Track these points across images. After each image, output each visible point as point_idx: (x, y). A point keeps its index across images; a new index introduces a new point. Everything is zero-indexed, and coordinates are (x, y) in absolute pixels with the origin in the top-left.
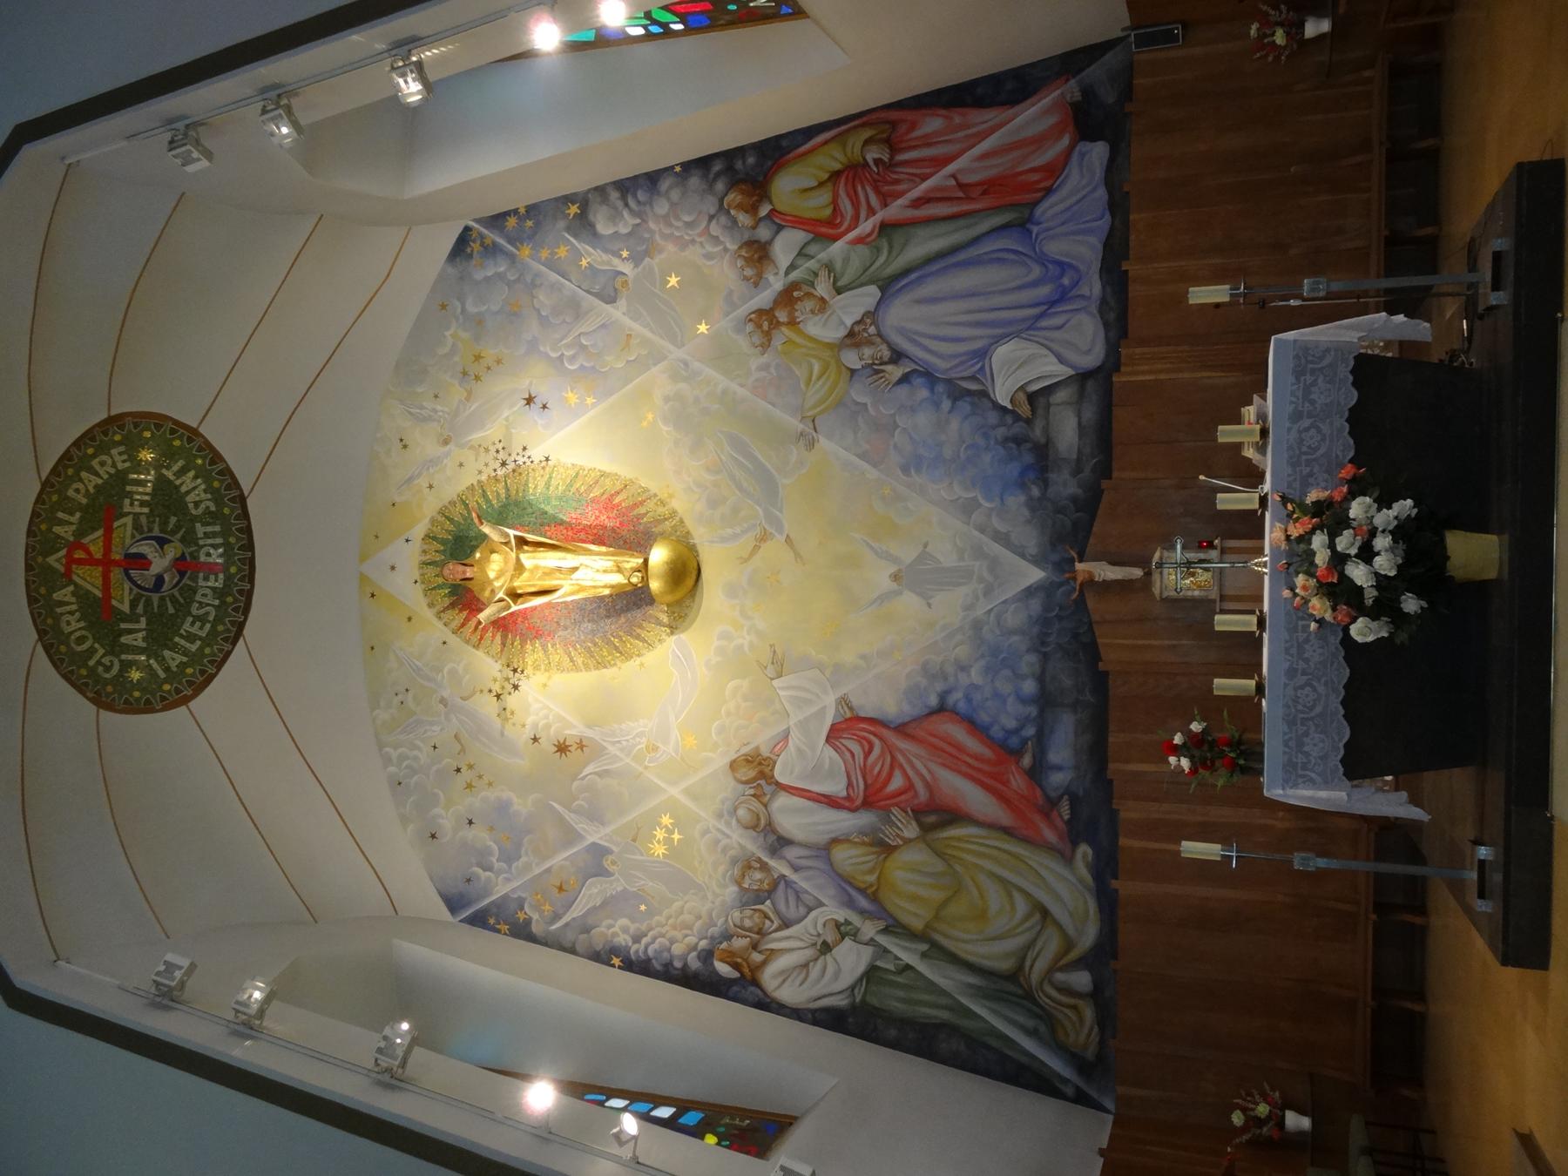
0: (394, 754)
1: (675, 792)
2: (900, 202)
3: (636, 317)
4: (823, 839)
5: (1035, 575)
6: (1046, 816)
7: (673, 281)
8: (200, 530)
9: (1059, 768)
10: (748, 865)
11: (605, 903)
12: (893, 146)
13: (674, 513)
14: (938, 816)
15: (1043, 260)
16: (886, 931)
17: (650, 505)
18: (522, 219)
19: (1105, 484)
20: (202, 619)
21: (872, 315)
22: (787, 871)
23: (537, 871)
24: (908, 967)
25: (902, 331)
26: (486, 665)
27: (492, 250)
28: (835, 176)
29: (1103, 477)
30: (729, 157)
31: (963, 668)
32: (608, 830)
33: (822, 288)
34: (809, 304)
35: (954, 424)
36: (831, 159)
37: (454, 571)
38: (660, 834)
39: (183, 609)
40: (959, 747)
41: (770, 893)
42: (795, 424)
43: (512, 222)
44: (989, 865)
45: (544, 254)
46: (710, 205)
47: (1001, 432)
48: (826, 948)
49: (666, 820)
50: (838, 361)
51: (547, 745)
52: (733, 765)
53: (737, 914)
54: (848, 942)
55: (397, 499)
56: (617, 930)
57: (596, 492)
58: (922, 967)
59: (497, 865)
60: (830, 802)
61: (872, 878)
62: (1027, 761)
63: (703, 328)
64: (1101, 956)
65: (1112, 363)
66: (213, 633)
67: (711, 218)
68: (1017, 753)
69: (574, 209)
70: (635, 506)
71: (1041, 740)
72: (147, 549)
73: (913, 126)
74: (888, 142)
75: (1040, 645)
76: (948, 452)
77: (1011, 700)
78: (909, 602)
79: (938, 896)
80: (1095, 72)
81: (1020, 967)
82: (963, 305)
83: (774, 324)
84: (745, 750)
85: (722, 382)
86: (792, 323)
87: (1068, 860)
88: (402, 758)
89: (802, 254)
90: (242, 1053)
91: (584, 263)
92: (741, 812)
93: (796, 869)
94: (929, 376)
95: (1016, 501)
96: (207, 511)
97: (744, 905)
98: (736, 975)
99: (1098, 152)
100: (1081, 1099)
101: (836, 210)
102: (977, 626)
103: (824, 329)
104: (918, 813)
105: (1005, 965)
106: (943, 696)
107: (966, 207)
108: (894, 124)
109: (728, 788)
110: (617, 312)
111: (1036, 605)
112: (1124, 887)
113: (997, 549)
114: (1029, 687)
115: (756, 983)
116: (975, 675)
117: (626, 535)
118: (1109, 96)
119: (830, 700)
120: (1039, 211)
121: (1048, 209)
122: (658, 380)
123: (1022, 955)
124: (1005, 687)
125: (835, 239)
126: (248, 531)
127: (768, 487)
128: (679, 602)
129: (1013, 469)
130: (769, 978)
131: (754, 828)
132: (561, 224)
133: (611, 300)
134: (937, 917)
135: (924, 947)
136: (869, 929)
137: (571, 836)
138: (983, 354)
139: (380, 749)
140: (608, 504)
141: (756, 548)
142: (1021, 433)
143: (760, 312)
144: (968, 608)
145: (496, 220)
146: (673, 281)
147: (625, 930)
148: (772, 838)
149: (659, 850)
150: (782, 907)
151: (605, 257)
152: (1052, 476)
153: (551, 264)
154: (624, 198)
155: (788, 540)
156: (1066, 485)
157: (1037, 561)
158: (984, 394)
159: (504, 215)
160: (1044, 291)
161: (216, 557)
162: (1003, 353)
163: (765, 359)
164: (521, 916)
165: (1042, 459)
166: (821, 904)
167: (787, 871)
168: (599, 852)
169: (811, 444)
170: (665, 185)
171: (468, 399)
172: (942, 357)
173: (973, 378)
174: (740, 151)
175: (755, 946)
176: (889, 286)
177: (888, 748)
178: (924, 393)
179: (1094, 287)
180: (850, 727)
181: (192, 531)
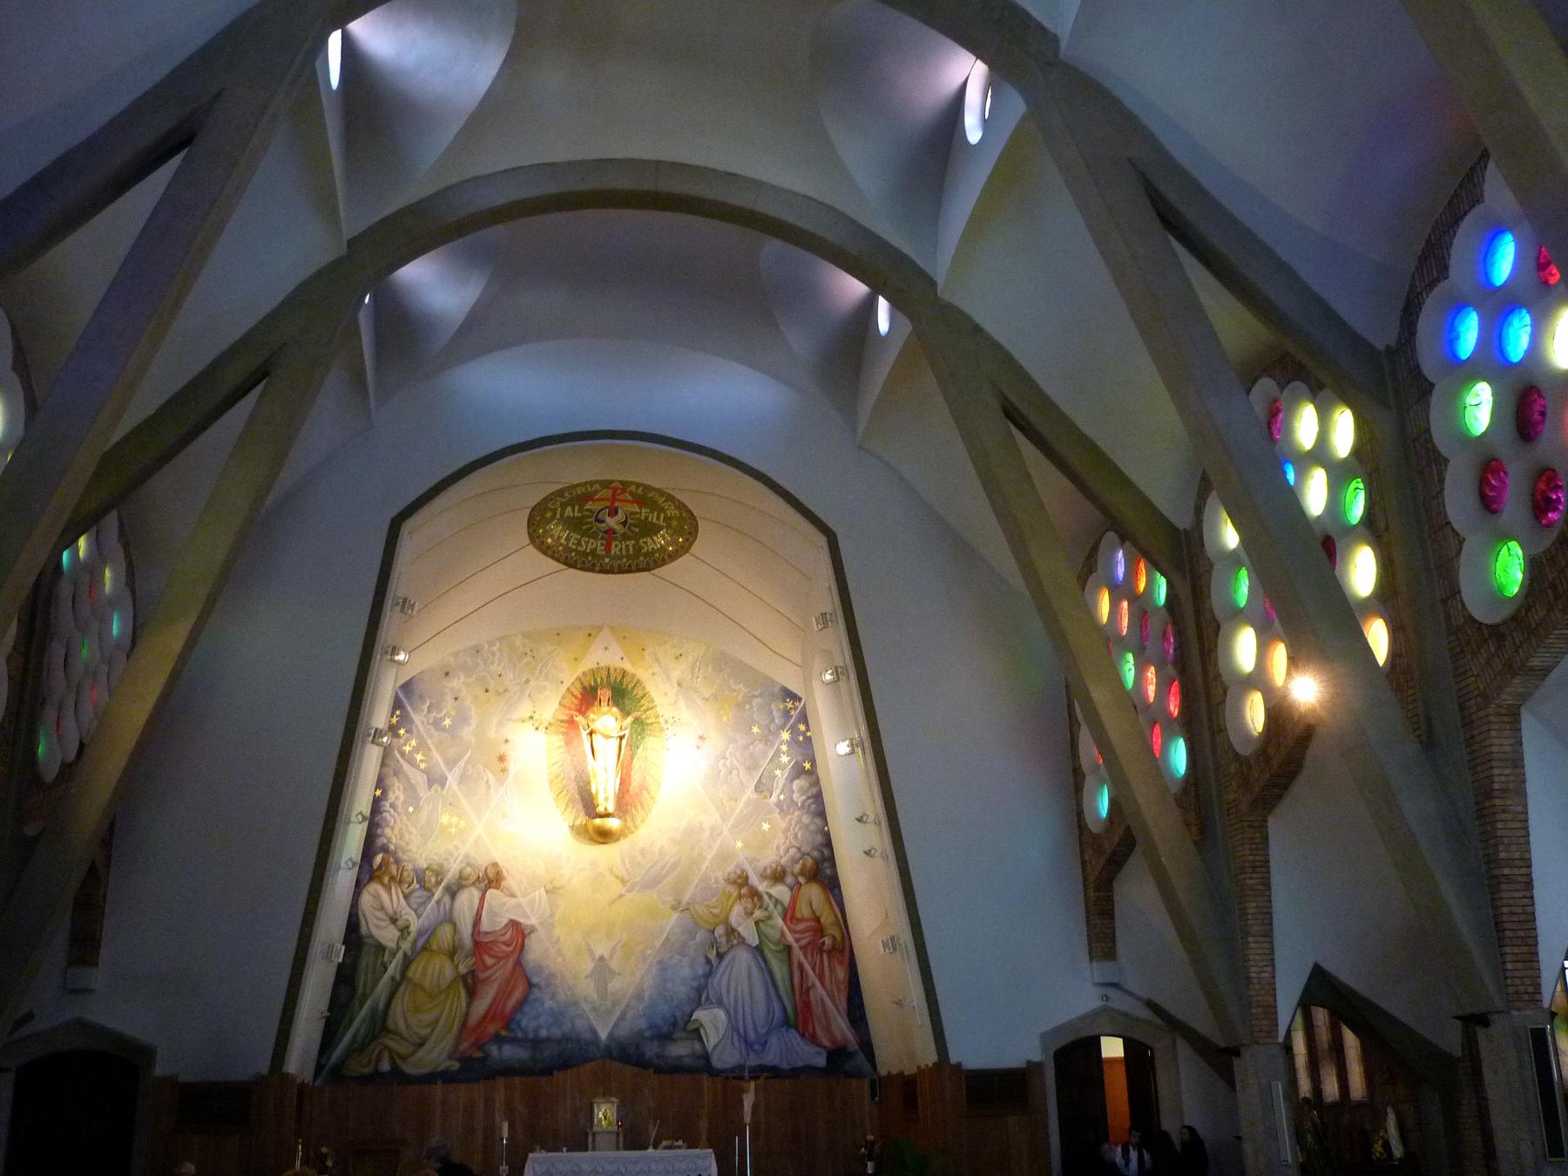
1: (479, 830)
3: (747, 804)
6: (474, 1044)
7: (766, 826)
9: (500, 1049)
10: (439, 873)
13: (637, 827)
14: (471, 984)
16: (405, 955)
18: (804, 734)
20: (579, 544)
21: (743, 941)
22: (436, 896)
24: (386, 970)
26: (550, 706)
27: (786, 714)
28: (818, 920)
29: (654, 1071)
30: (831, 859)
31: (553, 996)
33: (758, 914)
34: (749, 906)
36: (827, 918)
37: (604, 694)
38: (455, 820)
39: (585, 534)
40: (510, 994)
41: (423, 887)
42: (686, 897)
43: (802, 728)
45: (784, 748)
46: (806, 849)
47: (679, 1014)
48: (394, 921)
51: (503, 749)
52: (495, 865)
53: (410, 867)
54: (397, 933)
56: (397, 794)
57: (649, 779)
58: (387, 976)
60: (477, 922)
61: (435, 947)
62: (504, 1033)
63: (739, 844)
64: (398, 1075)
66: (572, 550)
68: (507, 1026)
69: (807, 766)
71: (513, 1040)
72: (621, 516)
73: (841, 963)
74: (834, 948)
75: (566, 1039)
76: (669, 985)
78: (589, 966)
79: (427, 985)
80: (861, 1058)
81: (389, 1032)
83: (740, 886)
84: (504, 873)
87: (450, 1057)
88: (493, 654)
89: (777, 902)
90: (377, 656)
91: (778, 772)
92: (469, 870)
93: (438, 902)
94: (709, 975)
95: (642, 1024)
96: (641, 548)
97: (415, 870)
99: (821, 1061)
100: (319, 1068)
102: (576, 1004)
103: (736, 915)
104: (472, 973)
105: (390, 1023)
106: (538, 986)
108: (842, 952)
109: (482, 861)
110: (750, 793)
111: (587, 1036)
112: (438, 1089)
114: (544, 1033)
115: (371, 879)
116: (549, 1003)
119: (533, 921)
120: (793, 1031)
121: (794, 1036)
122: (711, 818)
123: (396, 1033)
124: (542, 1020)
125: (784, 919)
126: (629, 571)
127: (651, 884)
128: (587, 831)
129: (660, 1022)
130: (374, 887)
131: (461, 877)
133: (757, 789)
135: (398, 977)
136: (406, 946)
137: (451, 764)
138: (720, 1003)
140: (643, 787)
141: (617, 877)
142: (678, 1025)
143: (747, 878)
145: (804, 718)
146: (766, 826)
149: (445, 819)
155: (622, 896)
156: (651, 1050)
157: (610, 1036)
158: (699, 1004)
159: (806, 723)
160: (752, 1036)
164: (402, 732)
165: (665, 1037)
167: (436, 896)
168: (442, 782)
169: (674, 908)
170: (818, 821)
172: (719, 981)
174: (834, 865)
175: (392, 878)
176: (759, 950)
177: (507, 956)
178: (700, 972)
179: (753, 1061)
180: (519, 932)
181: (629, 538)
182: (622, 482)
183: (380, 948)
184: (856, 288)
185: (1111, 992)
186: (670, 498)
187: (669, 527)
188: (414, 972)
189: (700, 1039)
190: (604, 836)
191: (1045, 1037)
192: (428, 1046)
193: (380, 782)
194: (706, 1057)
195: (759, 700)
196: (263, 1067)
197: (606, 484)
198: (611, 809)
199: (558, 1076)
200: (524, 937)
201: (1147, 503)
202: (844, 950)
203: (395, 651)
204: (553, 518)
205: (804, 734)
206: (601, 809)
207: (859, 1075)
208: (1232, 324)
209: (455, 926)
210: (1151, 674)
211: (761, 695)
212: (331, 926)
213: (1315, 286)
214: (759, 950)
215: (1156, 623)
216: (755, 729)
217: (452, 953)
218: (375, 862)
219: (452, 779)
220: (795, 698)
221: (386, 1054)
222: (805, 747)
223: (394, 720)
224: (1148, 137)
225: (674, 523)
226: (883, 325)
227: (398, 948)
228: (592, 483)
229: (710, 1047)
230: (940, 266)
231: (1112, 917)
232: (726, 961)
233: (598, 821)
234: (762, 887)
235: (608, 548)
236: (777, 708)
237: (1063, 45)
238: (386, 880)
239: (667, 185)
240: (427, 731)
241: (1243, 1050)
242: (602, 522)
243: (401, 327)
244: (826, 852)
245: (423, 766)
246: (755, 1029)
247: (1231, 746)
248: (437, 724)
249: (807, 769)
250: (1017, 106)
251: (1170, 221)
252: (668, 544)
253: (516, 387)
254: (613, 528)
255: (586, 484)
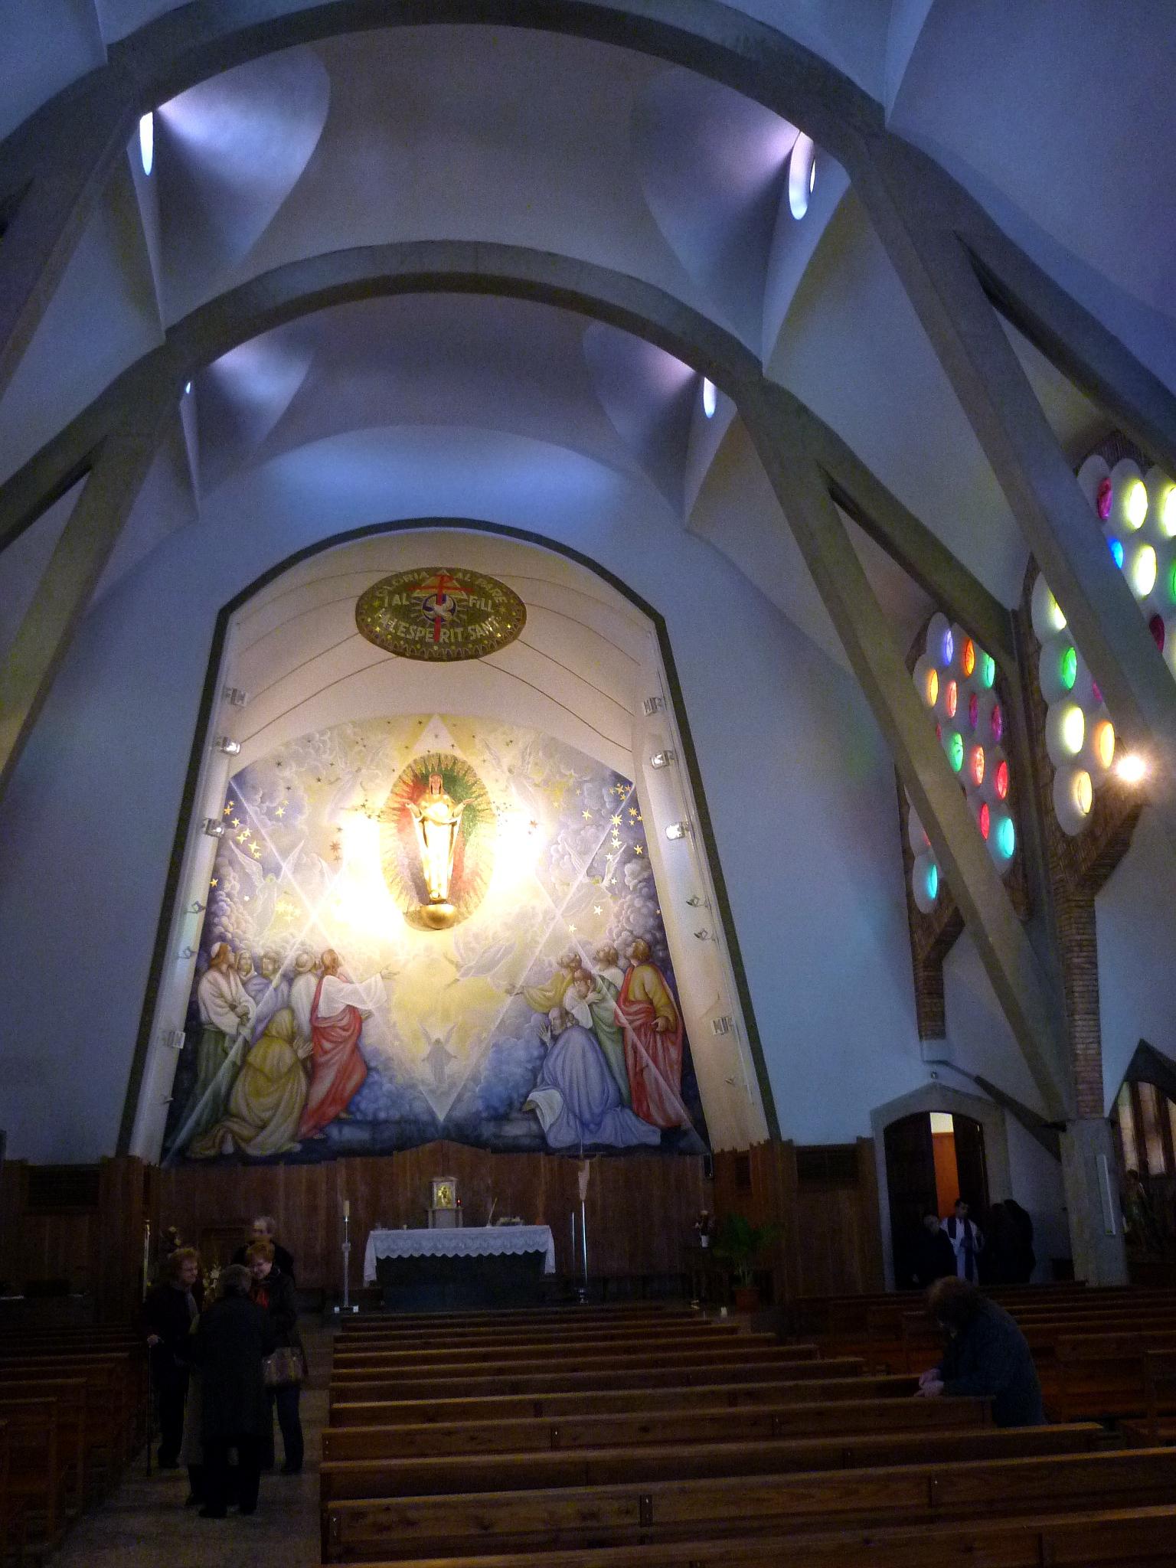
0: (326, 738)
2: (636, 1038)
4: (294, 1004)
5: (441, 1117)
6: (315, 1127)
7: (598, 910)
8: (459, 630)
9: (340, 1132)
10: (276, 961)
11: (247, 875)
12: (665, 1032)
13: (470, 913)
14: (311, 1068)
15: (603, 1113)
16: (246, 1041)
17: (475, 899)
18: (635, 818)
19: (489, 1150)
20: (407, 632)
21: (577, 1024)
22: (274, 983)
23: (263, 832)
24: (226, 1054)
25: (568, 1041)
27: (617, 799)
28: (651, 1002)
29: (490, 1147)
30: (663, 942)
31: (391, 1080)
32: (290, 876)
34: (583, 989)
35: (519, 1071)
36: (659, 1000)
37: (436, 781)
38: (290, 908)
40: (349, 1078)
41: (262, 975)
43: (633, 812)
44: (287, 1095)
45: (615, 832)
46: (638, 931)
47: (515, 1096)
48: (233, 1007)
49: (298, 912)
50: (551, 1007)
52: (331, 951)
54: (237, 1020)
55: (477, 740)
56: (232, 883)
58: (227, 1063)
59: (265, 806)
60: (315, 1008)
62: (343, 1115)
63: (572, 928)
64: (242, 1158)
65: (549, 1151)
67: (631, 932)
68: (347, 1110)
69: (639, 850)
70: (475, 890)
72: (449, 603)
73: (674, 1044)
75: (403, 1121)
76: (504, 1067)
77: (375, 1106)
78: (424, 1049)
79: (267, 1070)
80: (695, 1137)
82: (581, 1074)
83: (573, 970)
85: (543, 940)
86: (574, 980)
87: (293, 1138)
89: (610, 984)
90: (209, 748)
91: (609, 857)
92: (305, 957)
93: (275, 989)
94: (543, 1057)
95: (479, 1105)
98: (213, 955)
99: (655, 1139)
100: (165, 1151)
101: (633, 1003)
102: (413, 1086)
104: (311, 1058)
105: (232, 1106)
107: (631, 1073)
108: (675, 1032)
109: (318, 947)
110: (582, 877)
111: (425, 1118)
112: (281, 1170)
113: (454, 1096)
114: (382, 1115)
115: (210, 967)
116: (387, 1086)
117: (458, 887)
118: (682, 1144)
120: (628, 1111)
121: (628, 1116)
122: (543, 903)
124: (383, 1102)
126: (458, 658)
127: (485, 968)
128: (421, 918)
129: (496, 1103)
130: (213, 975)
131: (297, 964)
132: (631, 843)
133: (588, 874)
134: (256, 1070)
135: (239, 1063)
136: (246, 1032)
137: (285, 853)
138: (555, 1085)
139: (330, 729)
140: (476, 873)
141: (452, 962)
143: (580, 961)
144: (423, 1082)
145: (634, 802)
146: (598, 910)
147: (233, 888)
148: (292, 975)
150: (255, 981)
151: (612, 870)
152: (492, 1124)
153: (610, 835)
154: (645, 880)
156: (488, 1130)
157: (448, 1118)
158: (535, 1086)
160: (587, 1116)
161: (443, 638)
162: (556, 1095)
163: (555, 965)
164: (236, 822)
166: (257, 1004)
167: (274, 983)
168: (277, 871)
169: (509, 992)
170: (650, 904)
171: (536, 785)
173: (543, 1079)
174: (666, 948)
175: (230, 966)
176: (593, 1033)
177: (345, 1040)
178: (536, 1053)
179: (589, 1140)
180: (356, 1017)
182: (449, 570)
183: (221, 1034)
184: (680, 370)
185: (941, 1070)
186: (498, 585)
187: (497, 613)
188: (255, 1057)
189: (536, 1119)
190: (438, 922)
191: (876, 1114)
192: (269, 1129)
193: (216, 873)
194: (542, 1137)
195: (590, 785)
196: (111, 1153)
197: (433, 572)
198: (444, 896)
199: (397, 1157)
200: (361, 1022)
201: (975, 584)
202: (676, 1031)
203: (226, 742)
204: (381, 607)
205: (635, 818)
206: (434, 896)
207: (693, 1153)
208: (1060, 402)
209: (293, 1011)
210: (980, 755)
211: (591, 780)
212: (171, 1014)
213: (1145, 360)
214: (593, 1033)
215: (984, 704)
216: (586, 815)
217: (291, 1039)
218: (212, 950)
219: (286, 867)
220: (626, 782)
221: (229, 1137)
222: (636, 831)
223: (228, 811)
224: (977, 211)
225: (503, 610)
226: (709, 406)
227: (239, 1034)
228: (418, 571)
229: (546, 1128)
230: (765, 341)
231: (941, 996)
232: (561, 1043)
233: (432, 908)
234: (595, 970)
235: (436, 636)
236: (608, 793)
237: (888, 113)
238: (224, 967)
239: (492, 267)
240: (261, 821)
241: (1069, 1126)
242: (430, 609)
243: (223, 416)
244: (658, 935)
245: (257, 855)
246: (590, 1108)
247: (1058, 827)
248: (270, 814)
249: (638, 854)
250: (841, 180)
251: (996, 295)
252: (496, 630)
253: (341, 475)
254: (441, 613)
255: (412, 572)
